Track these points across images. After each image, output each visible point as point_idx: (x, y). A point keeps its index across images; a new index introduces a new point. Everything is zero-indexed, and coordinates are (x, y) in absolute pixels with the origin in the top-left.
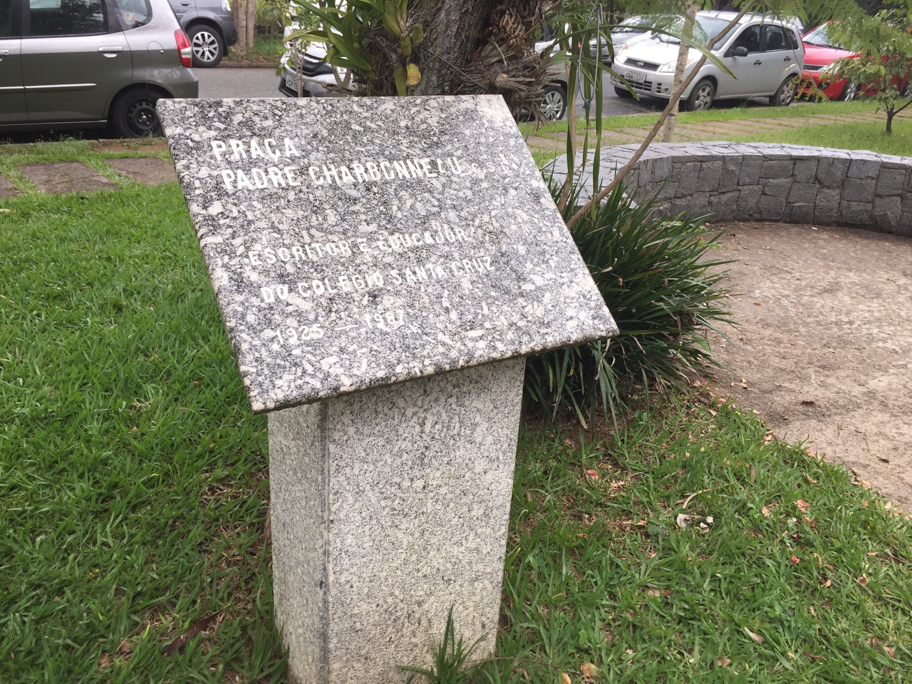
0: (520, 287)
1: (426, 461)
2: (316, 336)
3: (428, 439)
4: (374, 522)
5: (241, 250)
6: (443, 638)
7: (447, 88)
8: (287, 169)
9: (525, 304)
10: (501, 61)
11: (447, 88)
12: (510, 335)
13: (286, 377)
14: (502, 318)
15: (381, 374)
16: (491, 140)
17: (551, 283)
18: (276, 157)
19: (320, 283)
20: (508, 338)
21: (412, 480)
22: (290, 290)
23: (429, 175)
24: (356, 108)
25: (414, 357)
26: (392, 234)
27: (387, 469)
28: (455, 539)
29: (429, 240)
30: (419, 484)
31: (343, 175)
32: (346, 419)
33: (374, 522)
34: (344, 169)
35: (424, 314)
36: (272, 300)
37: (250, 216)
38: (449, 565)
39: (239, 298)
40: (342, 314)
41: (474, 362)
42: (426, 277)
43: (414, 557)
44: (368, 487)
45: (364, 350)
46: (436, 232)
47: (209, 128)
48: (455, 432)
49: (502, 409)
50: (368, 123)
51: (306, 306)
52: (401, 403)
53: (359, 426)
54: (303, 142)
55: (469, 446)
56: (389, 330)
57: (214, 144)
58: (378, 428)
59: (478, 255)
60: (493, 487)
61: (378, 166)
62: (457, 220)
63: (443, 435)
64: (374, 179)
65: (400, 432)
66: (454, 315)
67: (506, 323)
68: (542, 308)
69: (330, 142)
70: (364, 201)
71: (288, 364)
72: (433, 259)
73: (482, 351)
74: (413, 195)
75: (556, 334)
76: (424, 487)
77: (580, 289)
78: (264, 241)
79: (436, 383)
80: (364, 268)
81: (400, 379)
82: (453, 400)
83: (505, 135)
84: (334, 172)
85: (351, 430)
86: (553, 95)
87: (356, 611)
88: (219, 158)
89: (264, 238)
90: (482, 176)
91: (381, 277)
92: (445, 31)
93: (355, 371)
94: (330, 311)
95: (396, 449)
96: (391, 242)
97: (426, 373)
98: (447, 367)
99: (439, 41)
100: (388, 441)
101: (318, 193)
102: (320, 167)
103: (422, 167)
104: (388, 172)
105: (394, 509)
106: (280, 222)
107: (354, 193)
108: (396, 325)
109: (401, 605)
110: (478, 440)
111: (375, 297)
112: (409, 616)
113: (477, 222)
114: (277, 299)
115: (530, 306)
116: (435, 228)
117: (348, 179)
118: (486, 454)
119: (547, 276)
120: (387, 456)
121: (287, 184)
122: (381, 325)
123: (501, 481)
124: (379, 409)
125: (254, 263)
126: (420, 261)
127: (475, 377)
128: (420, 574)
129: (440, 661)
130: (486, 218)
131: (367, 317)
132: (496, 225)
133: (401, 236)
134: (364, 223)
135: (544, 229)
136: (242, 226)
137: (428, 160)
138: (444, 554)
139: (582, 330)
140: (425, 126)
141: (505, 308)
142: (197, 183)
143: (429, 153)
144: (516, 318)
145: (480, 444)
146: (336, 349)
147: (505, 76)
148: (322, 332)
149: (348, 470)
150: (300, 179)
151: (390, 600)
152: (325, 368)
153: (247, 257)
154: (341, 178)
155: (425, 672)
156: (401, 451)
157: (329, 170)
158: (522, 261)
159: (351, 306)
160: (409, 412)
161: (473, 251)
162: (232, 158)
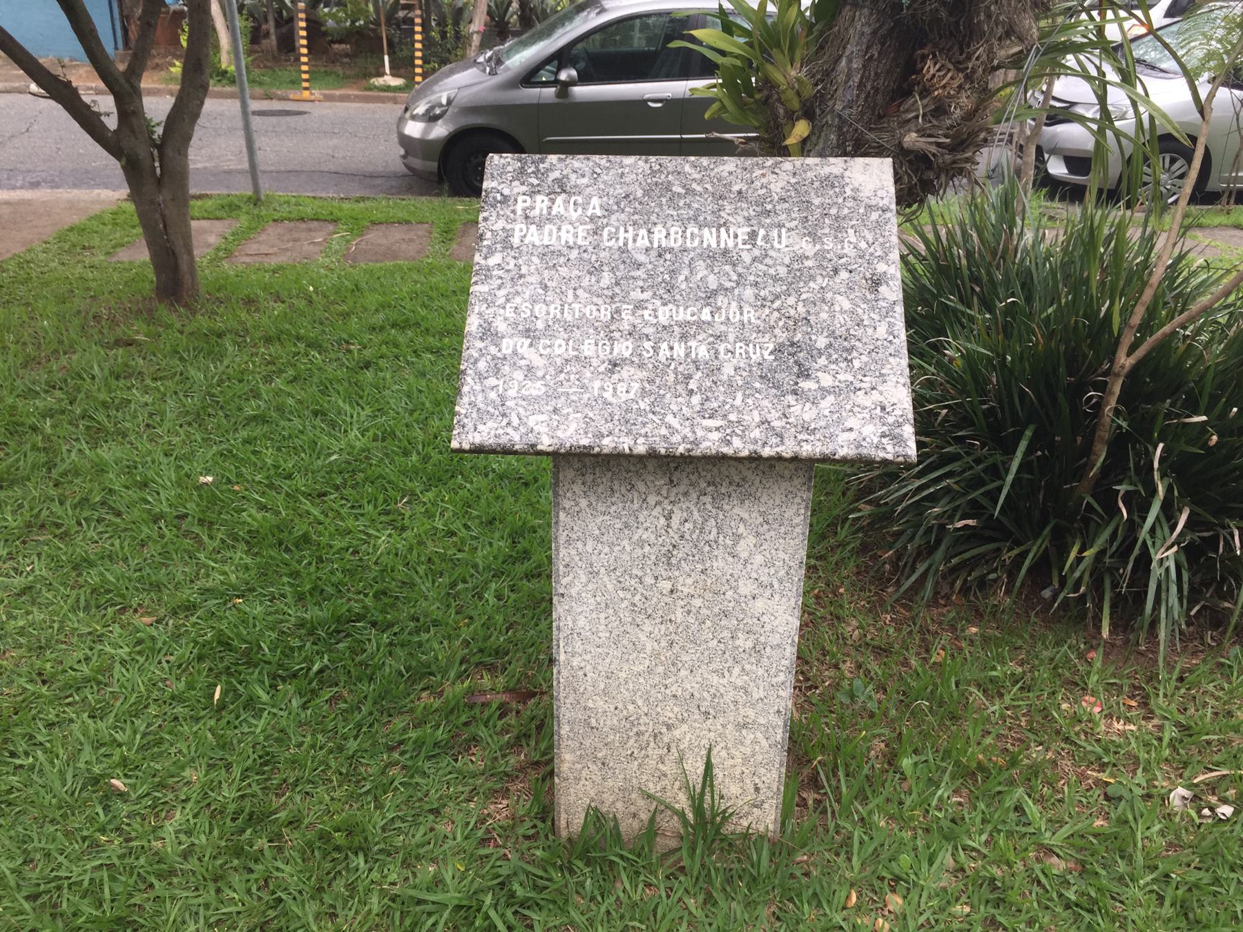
0: (797, 383)
1: (674, 561)
2: (535, 393)
3: (676, 537)
4: (611, 611)
5: (501, 301)
6: (700, 780)
7: (849, 149)
8: (581, 228)
9: (793, 403)
10: (917, 117)
11: (849, 149)
12: (756, 433)
13: (490, 424)
14: (756, 413)
15: (585, 442)
16: (846, 211)
17: (843, 385)
18: (574, 216)
19: (564, 343)
20: (752, 436)
21: (656, 578)
22: (531, 345)
23: (741, 246)
24: (687, 168)
25: (629, 433)
26: (665, 304)
27: (626, 557)
28: (713, 666)
29: (706, 315)
30: (667, 586)
31: (639, 239)
32: (577, 488)
33: (611, 611)
34: (643, 232)
35: (662, 392)
36: (510, 351)
37: (524, 270)
38: (706, 694)
39: (480, 344)
40: (572, 377)
41: (697, 453)
42: (682, 355)
43: (660, 669)
44: (603, 570)
45: (579, 415)
46: (719, 309)
47: (523, 184)
48: (712, 537)
49: (776, 526)
50: (694, 186)
51: (539, 362)
52: (641, 487)
53: (593, 499)
54: (611, 202)
55: (730, 559)
56: (614, 401)
57: (520, 198)
58: (614, 508)
59: (761, 340)
60: (764, 619)
61: (684, 232)
62: (752, 300)
63: (694, 536)
64: (672, 244)
65: (641, 519)
66: (696, 400)
67: (757, 419)
68: (815, 411)
69: (640, 203)
70: (650, 267)
71: (497, 413)
72: (700, 337)
73: (711, 443)
74: (710, 267)
75: (819, 444)
76: (672, 591)
77: (881, 399)
78: (527, 296)
79: (685, 474)
80: (617, 335)
81: (606, 451)
82: (708, 499)
83: (870, 207)
84: (630, 236)
85: (583, 503)
86: (1173, 161)
87: (590, 704)
88: (519, 212)
89: (528, 293)
90: (810, 253)
91: (631, 347)
92: (846, 82)
93: (559, 433)
94: (561, 372)
95: (636, 537)
96: (660, 313)
97: (635, 452)
98: (663, 451)
99: (840, 92)
100: (627, 526)
101: (603, 254)
102: (617, 229)
103: (736, 236)
104: (692, 239)
105: (635, 605)
106: (551, 279)
107: (642, 258)
108: (624, 397)
109: (644, 719)
110: (744, 555)
111: (615, 365)
112: (655, 736)
113: (777, 304)
114: (515, 353)
115: (799, 407)
116: (719, 304)
117: (643, 242)
118: (754, 575)
119: (841, 377)
120: (625, 543)
121: (575, 243)
122: (608, 395)
123: (781, 619)
124: (615, 488)
125: (508, 315)
126: (684, 337)
127: (737, 479)
128: (668, 691)
129: (697, 803)
130: (791, 300)
131: (597, 384)
132: (801, 309)
133: (674, 308)
134: (639, 290)
135: (866, 323)
136: (512, 279)
137: (749, 230)
138: (700, 679)
139: (859, 446)
140: (764, 191)
141: (766, 403)
142: (489, 235)
143: (753, 222)
144: (773, 416)
145: (746, 561)
146: (551, 409)
147: (914, 135)
148: (544, 389)
149: (580, 545)
150: (590, 239)
151: (631, 707)
152: (531, 423)
153: (504, 308)
154: (635, 241)
155: (675, 812)
156: (641, 543)
157: (626, 231)
158: (815, 353)
159: (586, 370)
160: (652, 499)
161: (755, 335)
162: (532, 214)
